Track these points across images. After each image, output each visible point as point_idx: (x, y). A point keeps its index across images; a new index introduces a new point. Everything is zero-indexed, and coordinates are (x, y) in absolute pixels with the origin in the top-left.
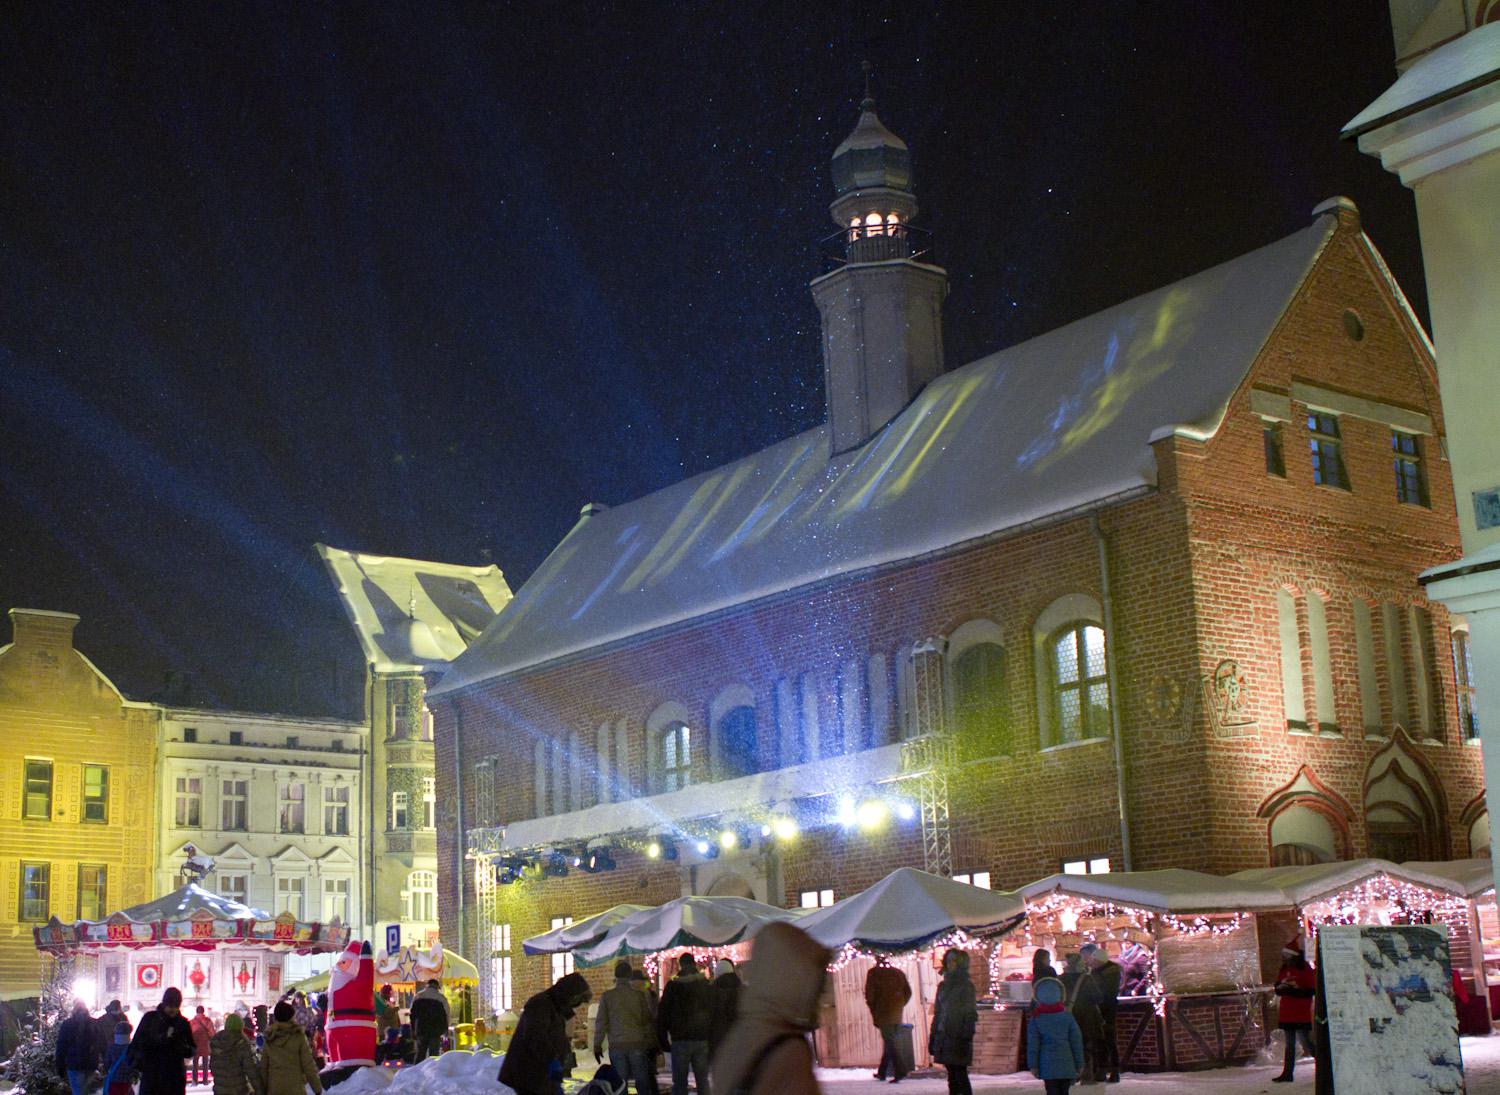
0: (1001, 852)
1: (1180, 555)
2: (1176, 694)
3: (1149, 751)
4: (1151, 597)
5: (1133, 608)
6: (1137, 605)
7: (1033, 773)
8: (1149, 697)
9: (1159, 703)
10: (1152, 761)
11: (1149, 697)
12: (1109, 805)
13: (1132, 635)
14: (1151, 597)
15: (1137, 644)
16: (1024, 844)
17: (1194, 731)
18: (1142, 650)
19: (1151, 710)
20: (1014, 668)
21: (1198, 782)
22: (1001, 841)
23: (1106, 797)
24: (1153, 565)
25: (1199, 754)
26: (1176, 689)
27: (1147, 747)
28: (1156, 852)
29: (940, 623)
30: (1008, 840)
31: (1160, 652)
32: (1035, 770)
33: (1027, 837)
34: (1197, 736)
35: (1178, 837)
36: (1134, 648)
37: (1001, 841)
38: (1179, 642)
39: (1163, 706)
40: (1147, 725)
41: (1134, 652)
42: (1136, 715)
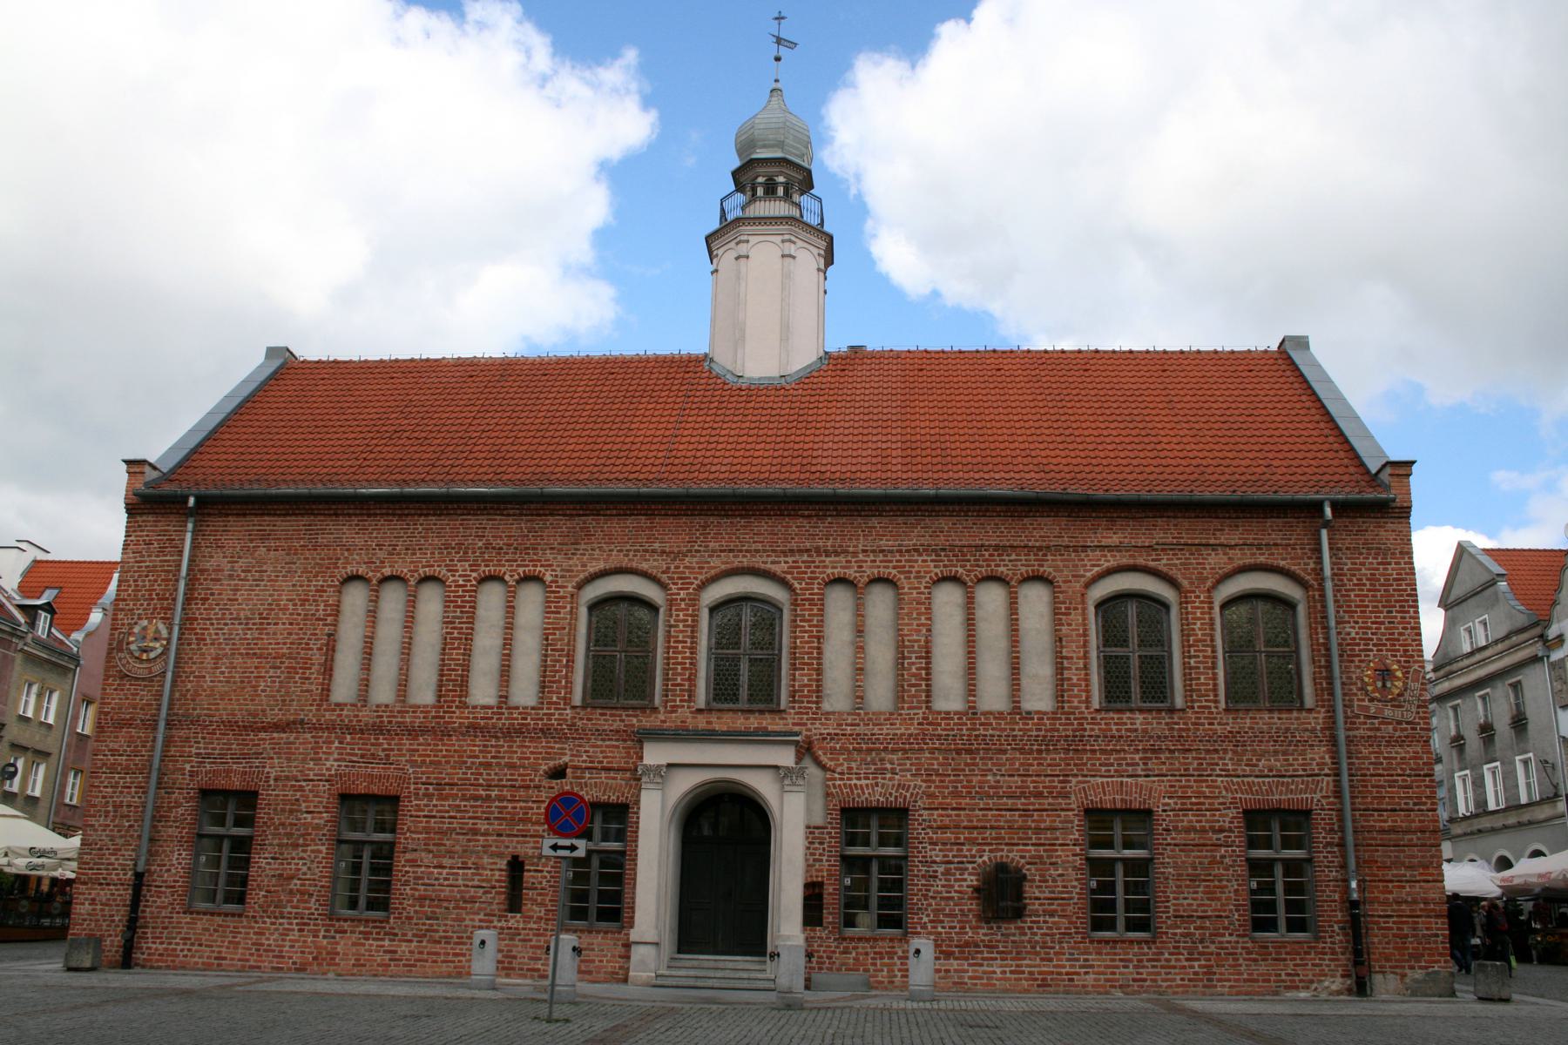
0: (1169, 798)
1: (1402, 561)
2: (1398, 679)
3: (1365, 723)
4: (1369, 590)
5: (1350, 596)
6: (1352, 594)
7: (1216, 726)
8: (1367, 676)
9: (1379, 684)
10: (1369, 733)
11: (1367, 676)
12: (1314, 767)
13: (1347, 619)
14: (1369, 590)
15: (1353, 628)
16: (1204, 792)
17: (1418, 713)
18: (1357, 633)
19: (1370, 688)
20: (1195, 624)
21: (1421, 758)
22: (1171, 786)
23: (1313, 759)
24: (1371, 563)
25: (1423, 733)
26: (1399, 674)
27: (1362, 720)
28: (1373, 815)
29: (1094, 565)
30: (1181, 787)
31: (1379, 639)
32: (1219, 724)
33: (1207, 787)
34: (1420, 718)
35: (1399, 804)
36: (1348, 630)
37: (1171, 786)
38: (1400, 634)
39: (1384, 685)
40: (1363, 700)
41: (1349, 634)
42: (1351, 690)
